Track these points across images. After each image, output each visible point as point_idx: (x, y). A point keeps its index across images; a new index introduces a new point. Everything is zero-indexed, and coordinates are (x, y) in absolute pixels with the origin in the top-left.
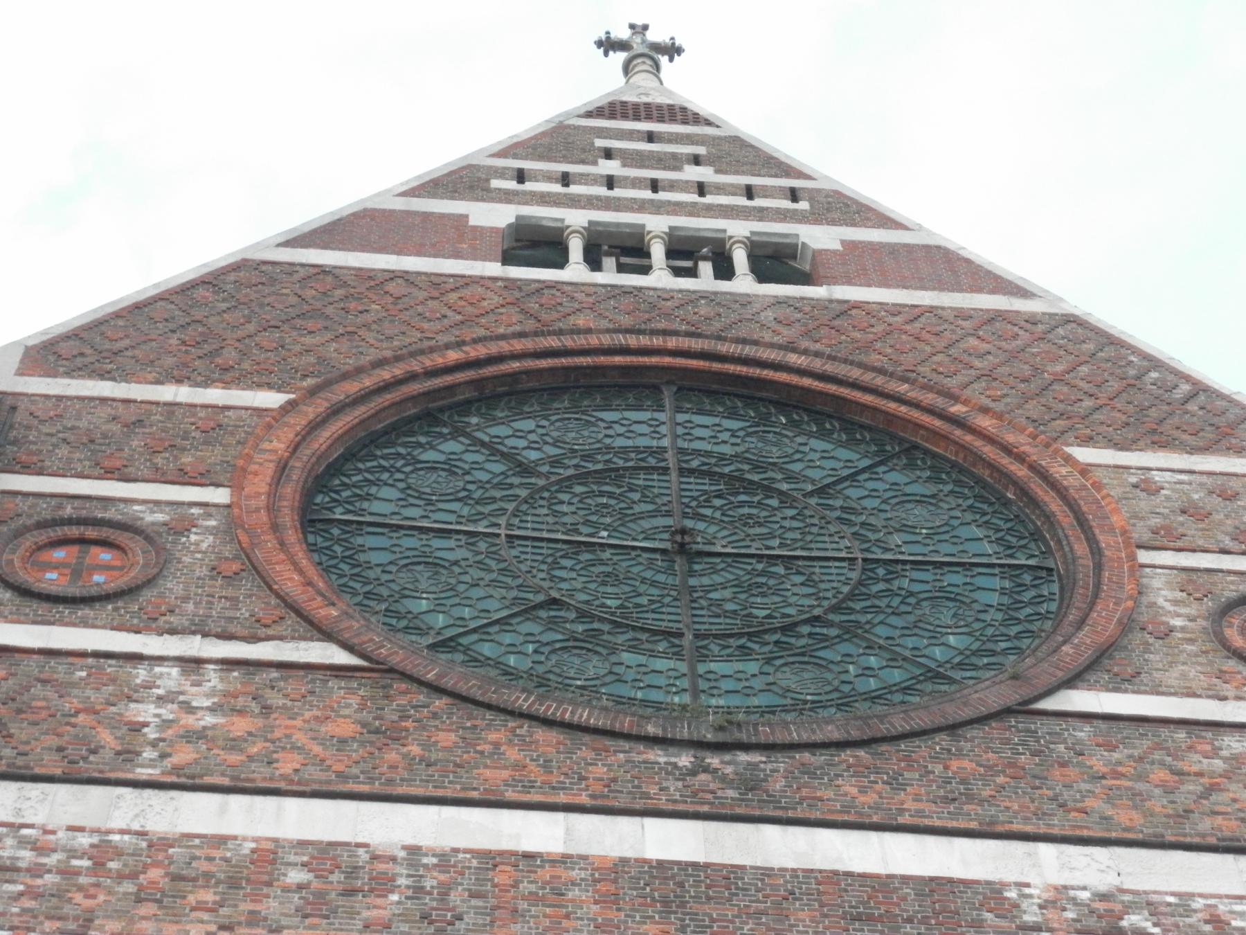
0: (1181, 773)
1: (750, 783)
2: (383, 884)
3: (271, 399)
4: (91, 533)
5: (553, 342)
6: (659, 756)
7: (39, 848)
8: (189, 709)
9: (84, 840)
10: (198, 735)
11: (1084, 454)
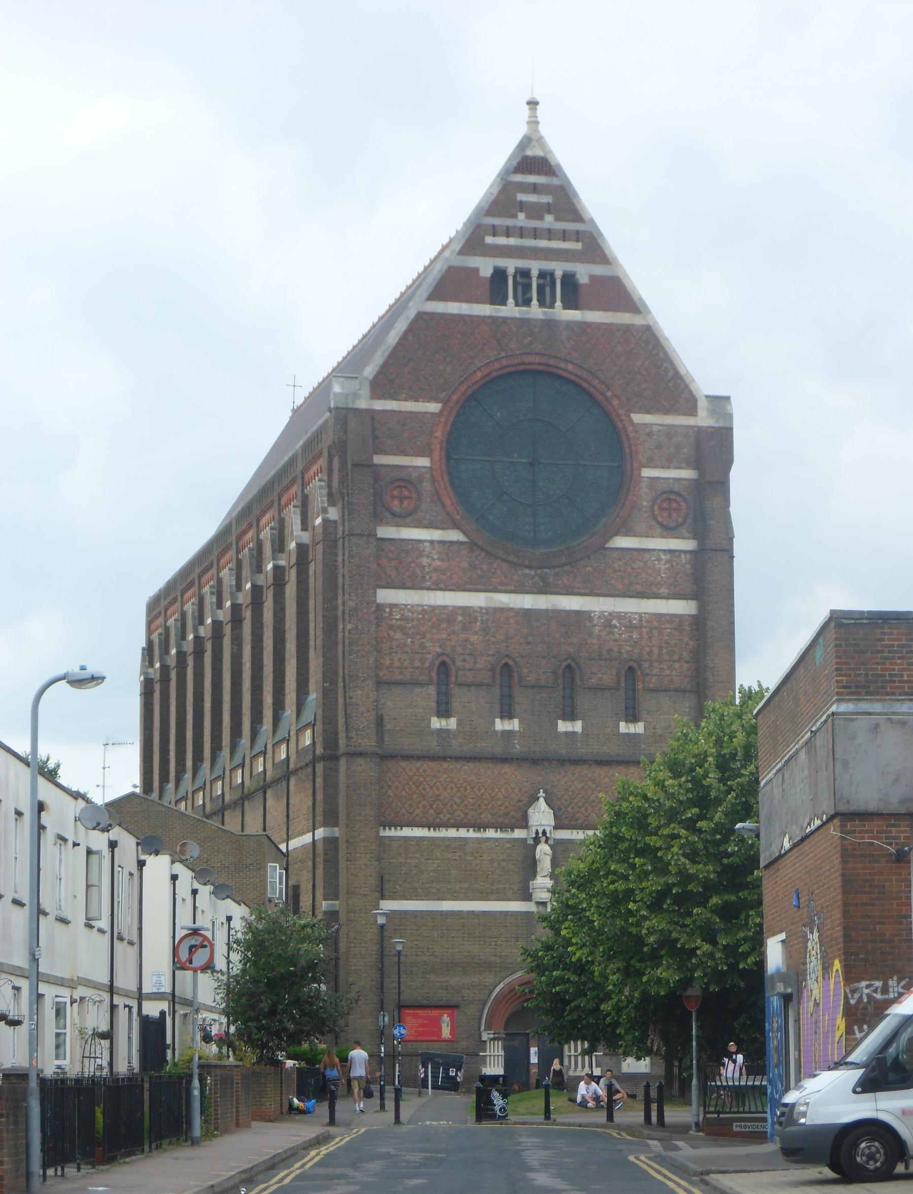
0: (633, 569)
2: (475, 620)
3: (434, 407)
4: (402, 484)
5: (504, 362)
6: (527, 571)
7: (413, 613)
8: (434, 560)
9: (420, 609)
10: (436, 570)
11: (637, 418)
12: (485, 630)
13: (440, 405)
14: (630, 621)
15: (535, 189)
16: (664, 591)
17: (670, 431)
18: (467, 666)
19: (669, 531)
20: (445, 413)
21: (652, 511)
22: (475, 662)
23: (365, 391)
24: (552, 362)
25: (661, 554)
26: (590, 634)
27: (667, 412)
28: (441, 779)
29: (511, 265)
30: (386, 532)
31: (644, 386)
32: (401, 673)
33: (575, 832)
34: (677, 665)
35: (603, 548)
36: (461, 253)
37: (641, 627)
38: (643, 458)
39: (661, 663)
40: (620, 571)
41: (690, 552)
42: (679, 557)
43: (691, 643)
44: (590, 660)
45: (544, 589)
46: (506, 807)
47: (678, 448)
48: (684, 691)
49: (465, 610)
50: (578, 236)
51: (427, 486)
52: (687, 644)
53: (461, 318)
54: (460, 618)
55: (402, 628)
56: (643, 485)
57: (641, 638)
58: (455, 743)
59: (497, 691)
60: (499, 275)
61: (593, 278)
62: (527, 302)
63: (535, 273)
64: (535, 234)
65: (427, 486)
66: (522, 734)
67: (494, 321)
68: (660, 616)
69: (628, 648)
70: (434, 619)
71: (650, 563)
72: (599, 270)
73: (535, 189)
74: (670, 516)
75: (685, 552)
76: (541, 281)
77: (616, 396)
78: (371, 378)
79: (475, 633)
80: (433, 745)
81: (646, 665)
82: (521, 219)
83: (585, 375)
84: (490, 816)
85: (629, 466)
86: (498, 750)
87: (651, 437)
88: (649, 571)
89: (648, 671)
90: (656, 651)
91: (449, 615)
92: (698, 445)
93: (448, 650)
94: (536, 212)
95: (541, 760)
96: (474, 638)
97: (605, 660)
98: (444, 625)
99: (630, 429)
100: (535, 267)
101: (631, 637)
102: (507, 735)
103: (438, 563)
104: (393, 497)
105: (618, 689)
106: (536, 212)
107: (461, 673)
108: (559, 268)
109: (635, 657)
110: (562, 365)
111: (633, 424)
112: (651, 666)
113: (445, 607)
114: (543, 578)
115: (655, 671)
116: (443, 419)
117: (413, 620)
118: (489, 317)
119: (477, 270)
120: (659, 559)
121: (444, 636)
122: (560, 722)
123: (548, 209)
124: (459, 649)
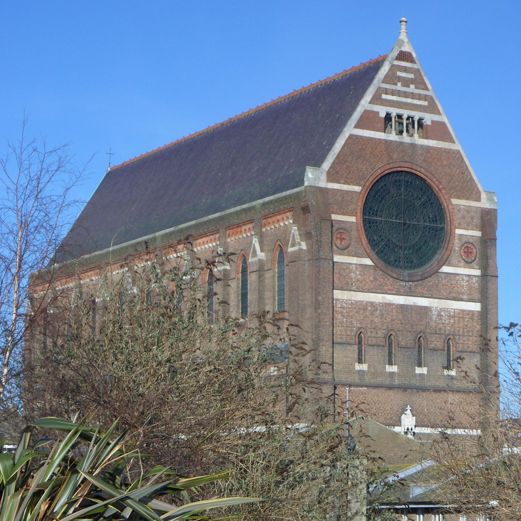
1: (410, 288)
2: (377, 310)
5: (391, 165)
6: (402, 283)
7: (347, 304)
9: (350, 302)
10: (358, 280)
11: (455, 201)
12: (382, 315)
13: (361, 188)
14: (450, 313)
15: (406, 70)
16: (465, 297)
17: (468, 209)
18: (372, 335)
19: (468, 264)
20: (363, 192)
21: (461, 253)
22: (377, 333)
23: (324, 177)
24: (414, 167)
25: (464, 277)
26: (431, 319)
27: (467, 199)
28: (360, 398)
29: (394, 111)
30: (337, 258)
31: (456, 184)
32: (341, 338)
33: (423, 428)
34: (471, 338)
35: (437, 272)
36: (370, 103)
37: (455, 317)
38: (456, 223)
39: (464, 336)
40: (445, 285)
41: (478, 276)
42: (472, 279)
43: (478, 326)
44: (431, 334)
45: (410, 293)
46: (391, 414)
47: (472, 218)
48: (474, 352)
49: (372, 304)
50: (425, 98)
51: (354, 233)
52: (476, 327)
53: (370, 139)
54: (369, 308)
55: (342, 313)
56: (456, 238)
57: (455, 323)
58: (367, 378)
59: (386, 349)
60: (388, 117)
61: (433, 122)
62: (401, 132)
63: (405, 117)
64: (406, 95)
65: (354, 233)
66: (399, 375)
67: (386, 141)
68: (463, 311)
69: (449, 328)
70: (357, 308)
71: (459, 282)
72: (436, 118)
73: (406, 70)
74: (468, 257)
75: (475, 276)
76: (408, 121)
77: (444, 188)
78: (327, 170)
79: (377, 317)
80: (356, 379)
81: (457, 338)
82: (399, 87)
83: (429, 175)
84: (383, 419)
85: (449, 227)
86: (387, 382)
87: (460, 212)
88: (459, 286)
89: (458, 341)
90: (461, 330)
91: (362, 307)
92: (482, 217)
93: (364, 326)
94: (406, 83)
95: (409, 388)
96: (376, 320)
97: (438, 334)
98: (362, 312)
99: (450, 207)
100: (406, 113)
101: (450, 322)
102: (392, 374)
103: (359, 277)
104: (337, 238)
105: (444, 351)
106: (406, 83)
107: (370, 339)
108: (417, 115)
109: (452, 333)
110: (419, 170)
111: (452, 204)
112: (459, 338)
113: (362, 301)
114: (410, 288)
115: (461, 341)
116: (362, 196)
117: (347, 308)
118: (384, 140)
119: (378, 113)
120: (463, 280)
121: (362, 318)
122: (416, 367)
123: (412, 81)
124: (369, 325)
